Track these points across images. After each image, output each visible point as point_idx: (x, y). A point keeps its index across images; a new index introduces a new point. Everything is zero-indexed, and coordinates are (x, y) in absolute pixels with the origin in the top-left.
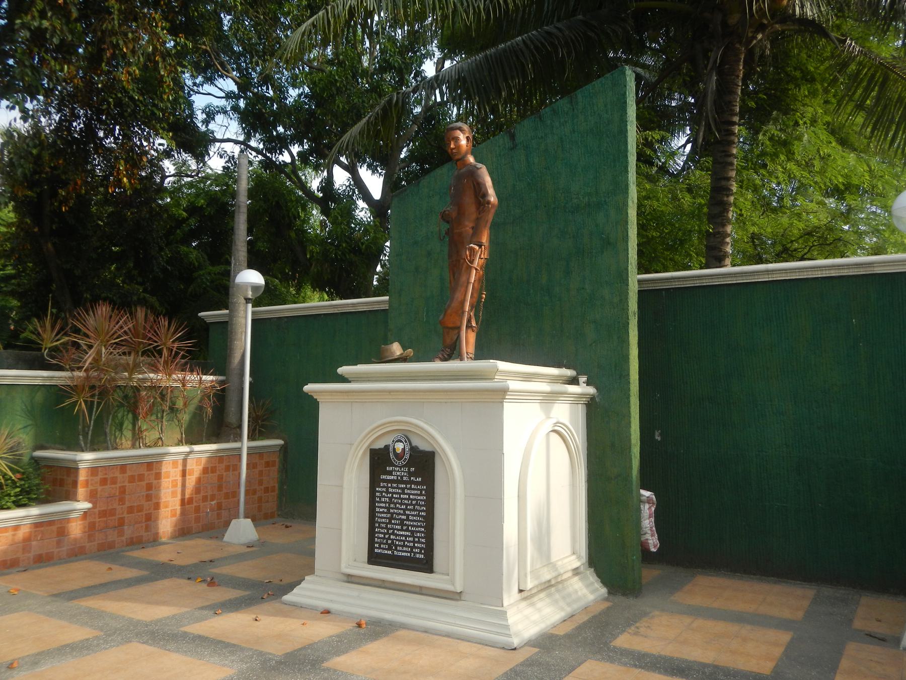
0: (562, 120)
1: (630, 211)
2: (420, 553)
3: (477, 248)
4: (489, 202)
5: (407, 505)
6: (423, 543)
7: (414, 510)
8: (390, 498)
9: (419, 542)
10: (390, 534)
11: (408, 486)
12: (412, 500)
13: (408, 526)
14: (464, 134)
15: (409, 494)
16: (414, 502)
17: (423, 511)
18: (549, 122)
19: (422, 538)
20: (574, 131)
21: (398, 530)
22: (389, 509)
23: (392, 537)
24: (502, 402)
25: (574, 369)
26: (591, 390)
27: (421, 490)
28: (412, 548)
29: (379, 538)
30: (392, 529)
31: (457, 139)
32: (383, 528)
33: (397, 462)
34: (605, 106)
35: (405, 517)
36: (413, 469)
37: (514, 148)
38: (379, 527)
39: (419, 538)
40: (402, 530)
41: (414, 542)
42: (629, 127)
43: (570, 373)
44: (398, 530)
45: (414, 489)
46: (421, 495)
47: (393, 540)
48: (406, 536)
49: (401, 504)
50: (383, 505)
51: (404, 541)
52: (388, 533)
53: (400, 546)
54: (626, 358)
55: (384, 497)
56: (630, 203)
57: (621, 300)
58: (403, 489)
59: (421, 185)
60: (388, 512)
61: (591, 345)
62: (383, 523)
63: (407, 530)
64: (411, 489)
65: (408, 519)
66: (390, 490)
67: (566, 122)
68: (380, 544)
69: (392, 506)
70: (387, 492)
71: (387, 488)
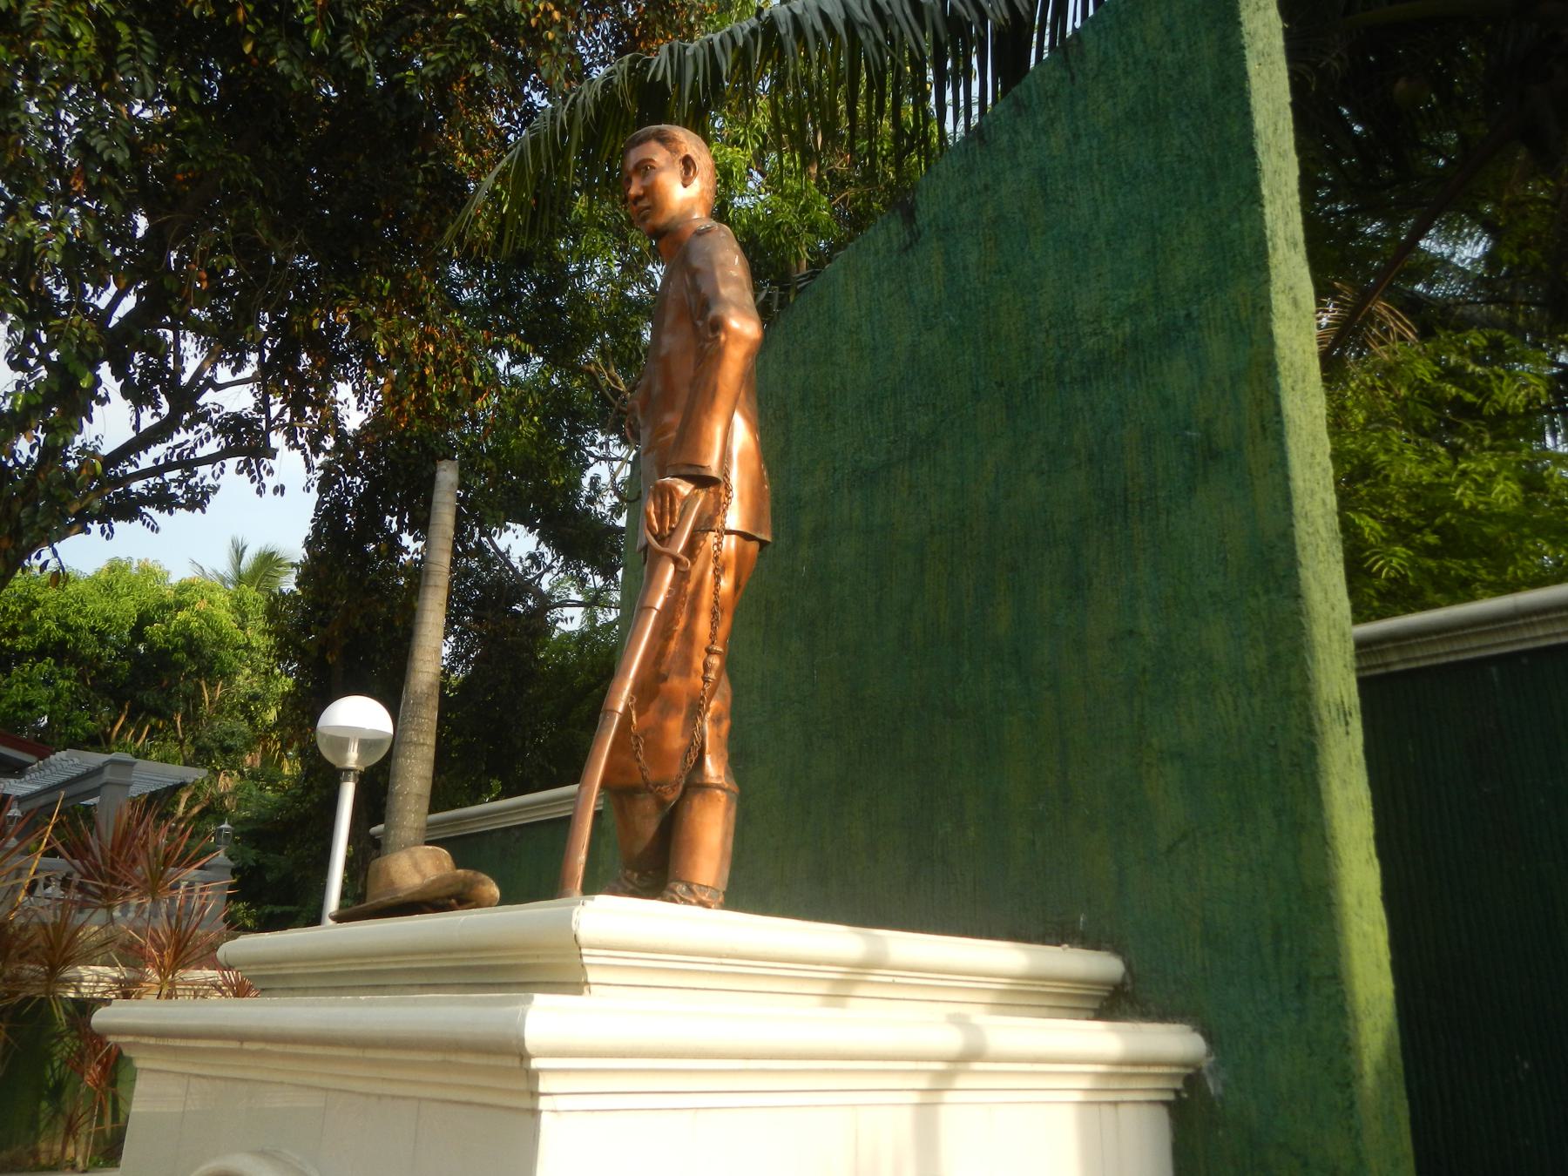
0: (1041, 120)
1: (1280, 329)
3: (685, 488)
4: (718, 325)
14: (675, 151)
18: (1005, 137)
20: (1077, 136)
24: (535, 1113)
25: (1117, 949)
26: (1175, 1042)
31: (645, 168)
34: (1169, 30)
37: (914, 240)
42: (1252, 66)
43: (1101, 965)
54: (1317, 901)
56: (1280, 303)
57: (1274, 661)
61: (1171, 849)
67: (1052, 121)
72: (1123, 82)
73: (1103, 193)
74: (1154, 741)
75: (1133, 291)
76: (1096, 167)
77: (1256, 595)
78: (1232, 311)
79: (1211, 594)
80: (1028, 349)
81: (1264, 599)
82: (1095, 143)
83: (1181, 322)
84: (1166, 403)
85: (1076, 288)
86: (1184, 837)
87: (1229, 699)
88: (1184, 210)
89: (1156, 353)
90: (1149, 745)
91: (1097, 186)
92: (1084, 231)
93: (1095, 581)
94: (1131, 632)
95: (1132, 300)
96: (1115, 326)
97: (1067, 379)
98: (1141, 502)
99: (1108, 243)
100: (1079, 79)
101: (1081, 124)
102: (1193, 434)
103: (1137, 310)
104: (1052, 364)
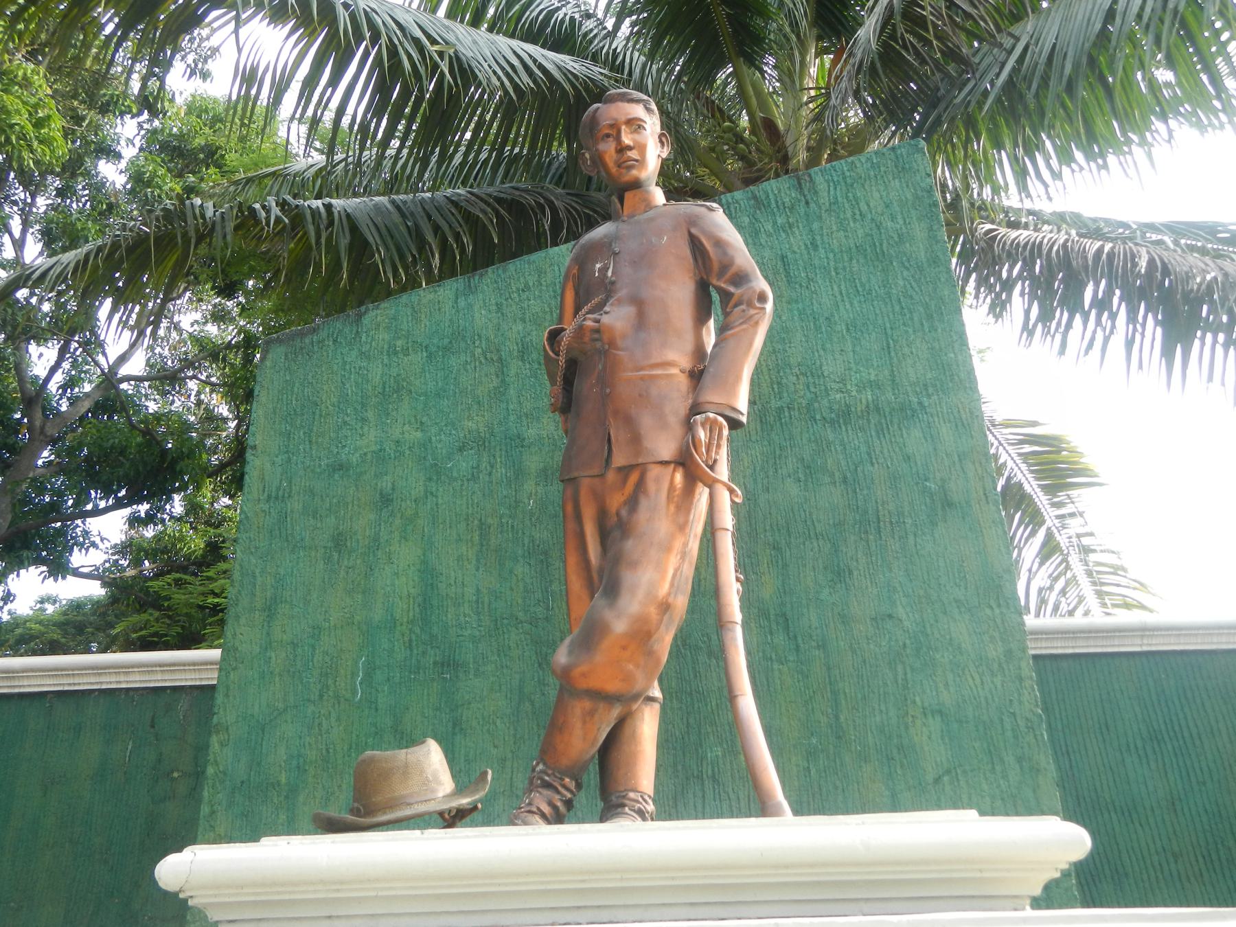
0: (780, 221)
59: (366, 320)
61: (937, 780)
72: (852, 224)
73: (841, 293)
74: (917, 699)
75: (873, 373)
76: (833, 273)
77: (991, 607)
78: (955, 411)
79: (956, 601)
80: (779, 383)
81: (997, 611)
82: (831, 256)
83: (916, 406)
84: (908, 458)
85: (822, 352)
86: (948, 772)
87: (977, 677)
88: (911, 331)
89: (895, 420)
90: (914, 702)
91: (835, 288)
92: (826, 315)
93: (855, 573)
94: (890, 616)
95: (873, 378)
96: (859, 391)
97: (818, 417)
98: (891, 523)
99: (848, 330)
100: (812, 205)
101: (818, 238)
102: (931, 485)
103: (875, 385)
104: (804, 402)
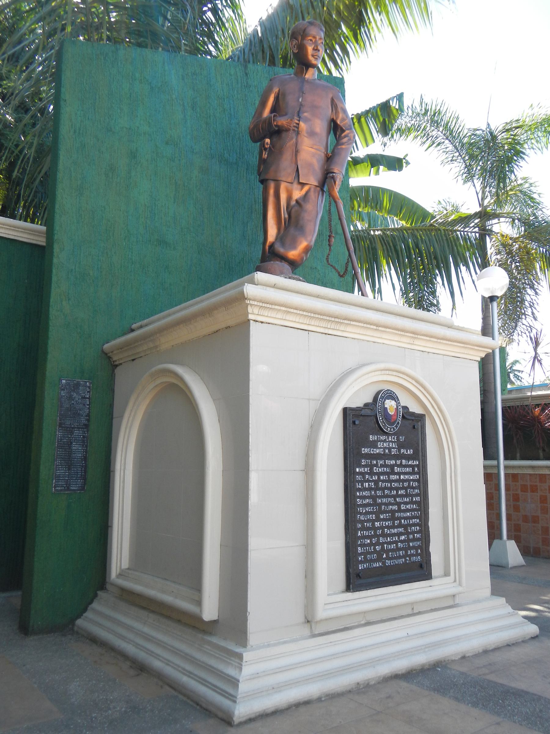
2: (417, 555)
5: (397, 489)
6: (418, 540)
7: (406, 496)
8: (376, 482)
9: (414, 540)
10: (378, 536)
11: (398, 462)
12: (404, 481)
13: (400, 519)
15: (399, 474)
16: (406, 484)
17: (417, 495)
19: (417, 532)
21: (388, 527)
22: (374, 498)
23: (381, 540)
27: (413, 466)
28: (406, 549)
29: (362, 545)
30: (382, 528)
32: (368, 529)
33: (388, 429)
35: (395, 507)
36: (402, 439)
38: (363, 529)
39: (413, 533)
40: (393, 527)
41: (408, 541)
44: (388, 527)
45: (406, 466)
46: (413, 473)
47: (383, 543)
48: (399, 534)
49: (391, 489)
50: (366, 493)
51: (396, 542)
52: (376, 535)
53: (392, 550)
55: (368, 481)
58: (392, 467)
60: (375, 504)
62: (368, 521)
63: (400, 526)
64: (401, 465)
65: (400, 510)
66: (376, 470)
68: (365, 554)
69: (379, 493)
70: (371, 473)
71: (371, 466)
